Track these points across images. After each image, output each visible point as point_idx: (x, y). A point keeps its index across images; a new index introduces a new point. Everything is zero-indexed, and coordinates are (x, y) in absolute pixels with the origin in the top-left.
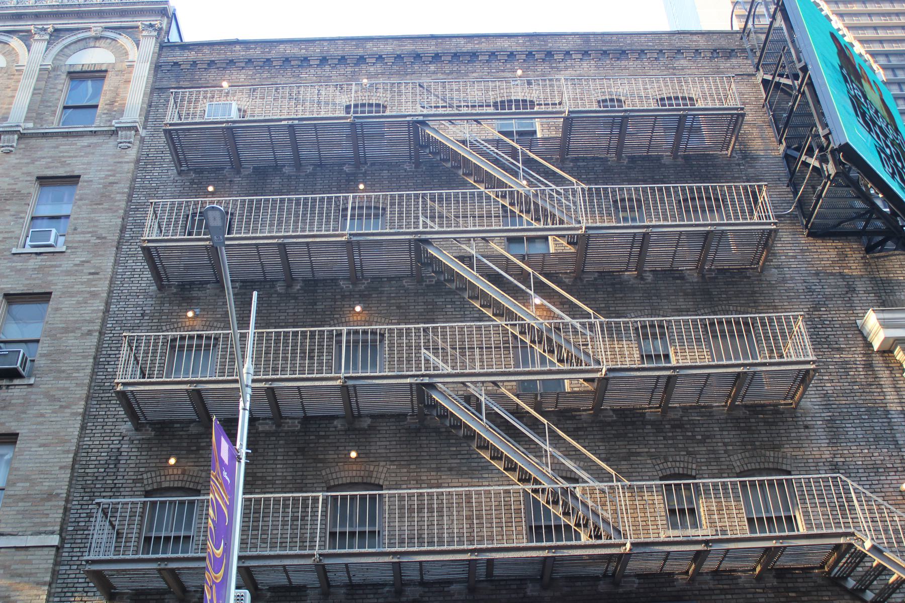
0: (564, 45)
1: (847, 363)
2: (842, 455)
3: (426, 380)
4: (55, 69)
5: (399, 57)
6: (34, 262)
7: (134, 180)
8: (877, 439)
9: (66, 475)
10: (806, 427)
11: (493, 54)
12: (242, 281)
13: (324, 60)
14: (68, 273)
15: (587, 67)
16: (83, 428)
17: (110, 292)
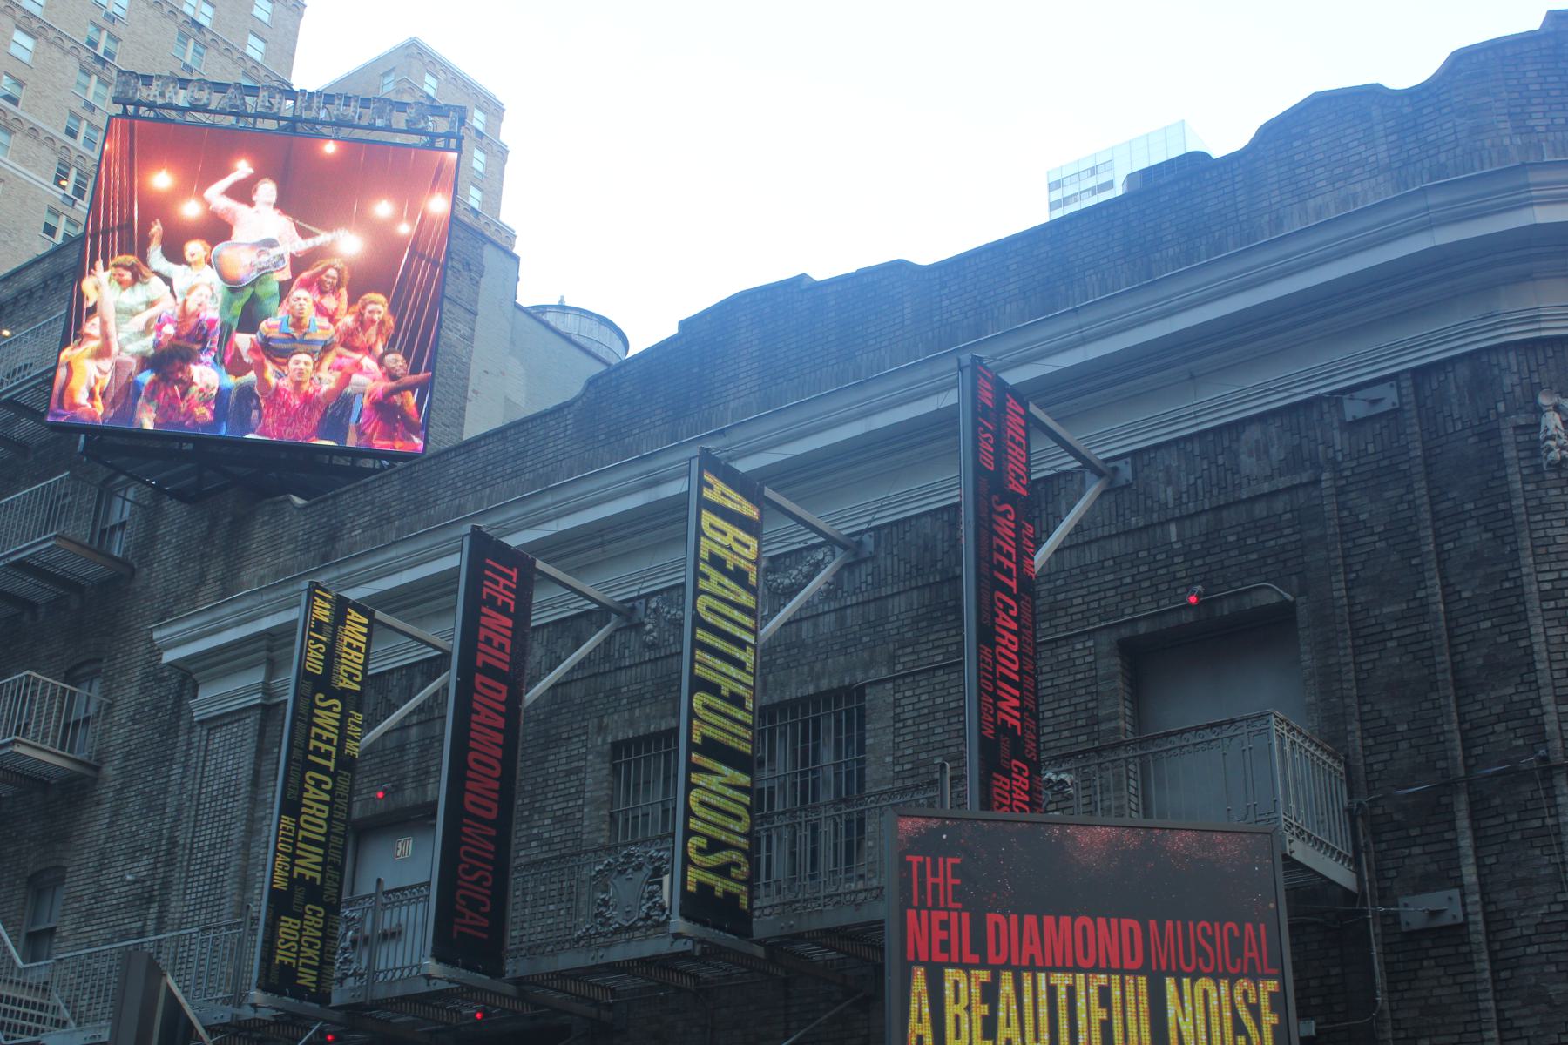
10: (98, 803)
11: (16, 300)
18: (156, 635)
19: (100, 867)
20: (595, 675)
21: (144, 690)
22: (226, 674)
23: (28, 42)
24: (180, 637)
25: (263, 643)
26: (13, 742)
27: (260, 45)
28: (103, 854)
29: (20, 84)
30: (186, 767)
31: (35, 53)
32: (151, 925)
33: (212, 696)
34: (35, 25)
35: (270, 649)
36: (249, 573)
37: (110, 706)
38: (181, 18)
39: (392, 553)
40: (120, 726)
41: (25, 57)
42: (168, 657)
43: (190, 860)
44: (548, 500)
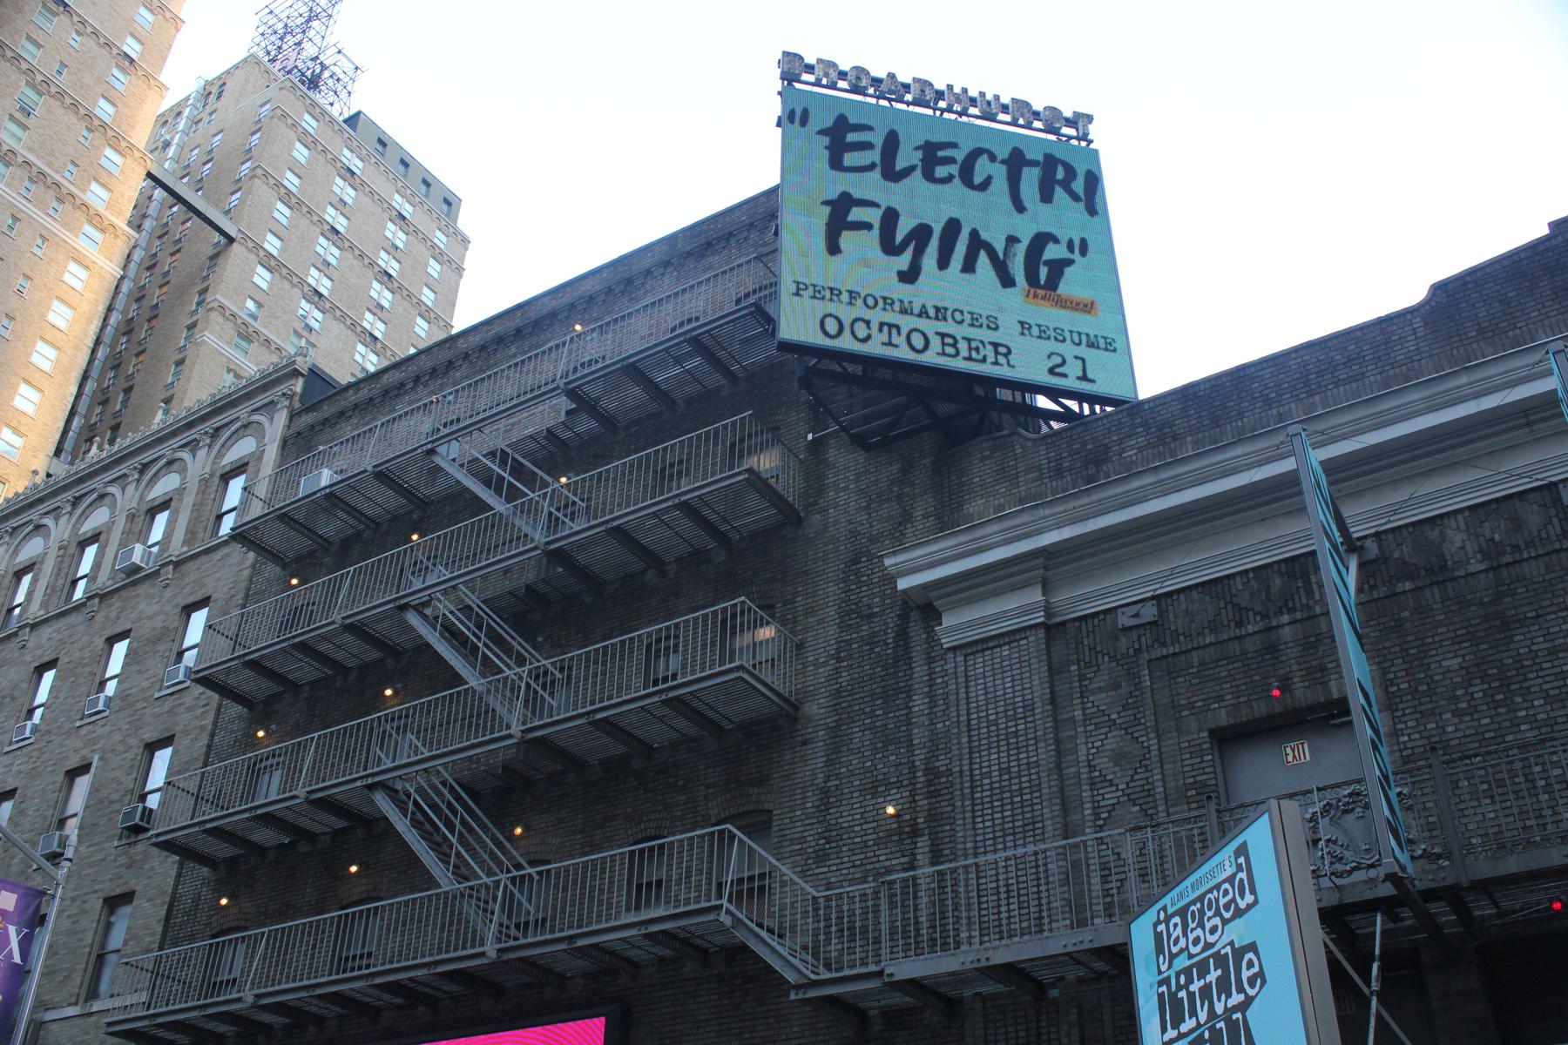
0: (645, 264)
1: (875, 634)
2: (838, 776)
3: (370, 781)
4: (212, 476)
5: (483, 348)
6: (169, 704)
7: (248, 589)
8: (887, 743)
9: (160, 929)
10: (804, 743)
11: (572, 306)
12: (312, 683)
13: (417, 379)
14: (189, 709)
15: (668, 285)
16: (179, 875)
17: (215, 724)
18: (888, 562)
19: (825, 805)
20: (1557, 551)
21: (843, 626)
22: (995, 594)
23: (267, 275)
24: (922, 562)
25: (1040, 561)
26: (739, 668)
27: (432, 295)
28: (826, 793)
29: (259, 305)
30: (931, 696)
31: (271, 284)
32: (922, 857)
33: (957, 623)
34: (273, 263)
35: (1046, 569)
36: (975, 506)
37: (800, 646)
38: (377, 269)
39: (1239, 451)
40: (817, 665)
41: (264, 286)
42: (903, 584)
43: (972, 788)
44: (1464, 379)
